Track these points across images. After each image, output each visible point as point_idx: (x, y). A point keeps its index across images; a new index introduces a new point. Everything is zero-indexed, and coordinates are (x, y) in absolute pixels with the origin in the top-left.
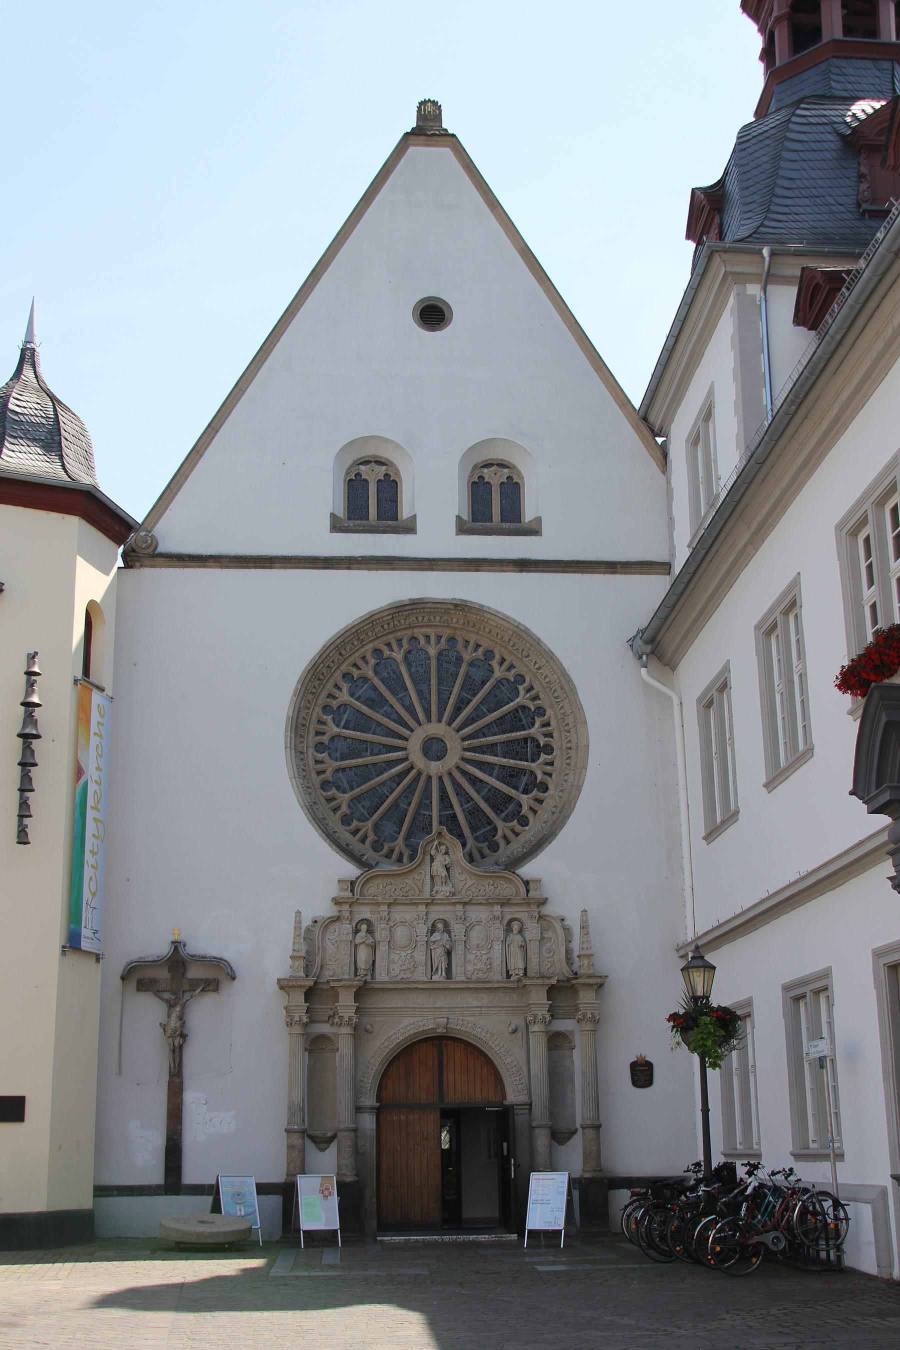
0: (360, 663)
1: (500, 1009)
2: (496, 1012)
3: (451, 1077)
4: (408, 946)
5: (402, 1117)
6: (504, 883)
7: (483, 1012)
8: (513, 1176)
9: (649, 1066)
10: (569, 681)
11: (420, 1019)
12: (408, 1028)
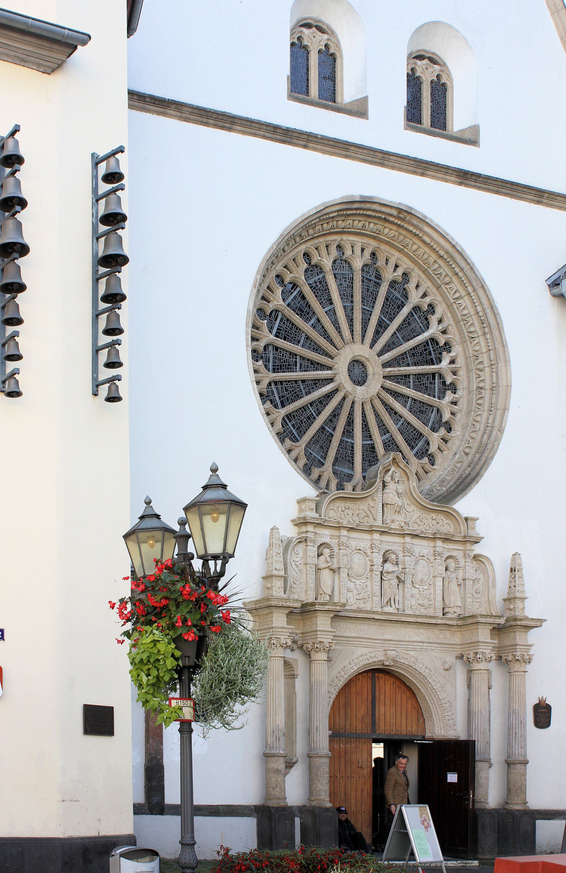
0: (292, 265)
1: (437, 645)
2: (434, 648)
3: (382, 709)
4: (361, 576)
5: (342, 746)
6: (444, 519)
7: (424, 647)
8: (471, 807)
9: (548, 708)
10: (495, 314)
11: (372, 650)
12: (361, 659)
